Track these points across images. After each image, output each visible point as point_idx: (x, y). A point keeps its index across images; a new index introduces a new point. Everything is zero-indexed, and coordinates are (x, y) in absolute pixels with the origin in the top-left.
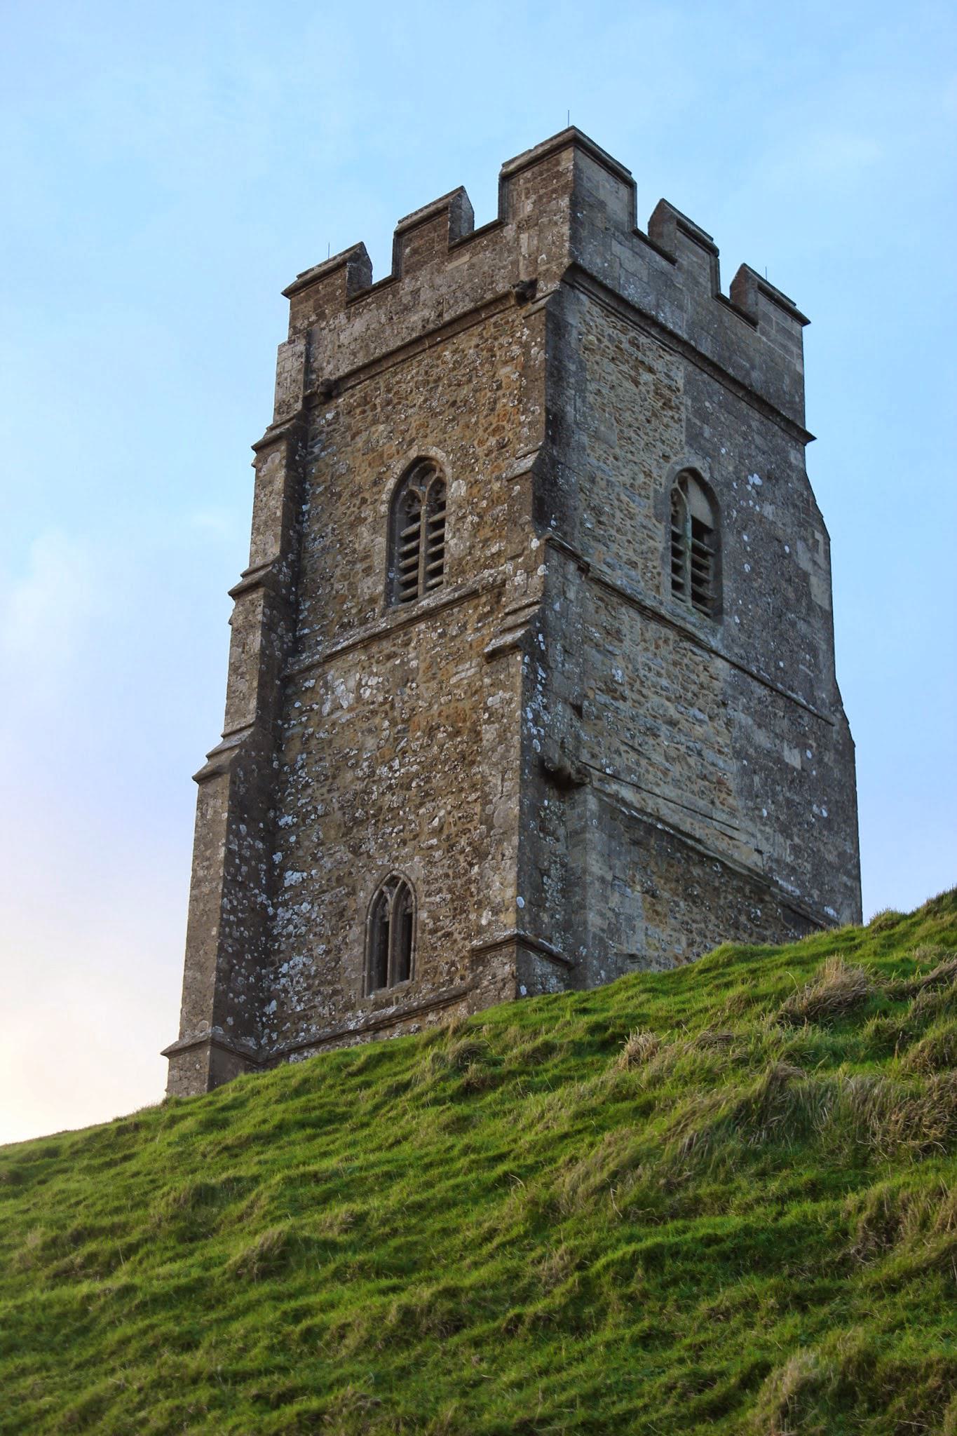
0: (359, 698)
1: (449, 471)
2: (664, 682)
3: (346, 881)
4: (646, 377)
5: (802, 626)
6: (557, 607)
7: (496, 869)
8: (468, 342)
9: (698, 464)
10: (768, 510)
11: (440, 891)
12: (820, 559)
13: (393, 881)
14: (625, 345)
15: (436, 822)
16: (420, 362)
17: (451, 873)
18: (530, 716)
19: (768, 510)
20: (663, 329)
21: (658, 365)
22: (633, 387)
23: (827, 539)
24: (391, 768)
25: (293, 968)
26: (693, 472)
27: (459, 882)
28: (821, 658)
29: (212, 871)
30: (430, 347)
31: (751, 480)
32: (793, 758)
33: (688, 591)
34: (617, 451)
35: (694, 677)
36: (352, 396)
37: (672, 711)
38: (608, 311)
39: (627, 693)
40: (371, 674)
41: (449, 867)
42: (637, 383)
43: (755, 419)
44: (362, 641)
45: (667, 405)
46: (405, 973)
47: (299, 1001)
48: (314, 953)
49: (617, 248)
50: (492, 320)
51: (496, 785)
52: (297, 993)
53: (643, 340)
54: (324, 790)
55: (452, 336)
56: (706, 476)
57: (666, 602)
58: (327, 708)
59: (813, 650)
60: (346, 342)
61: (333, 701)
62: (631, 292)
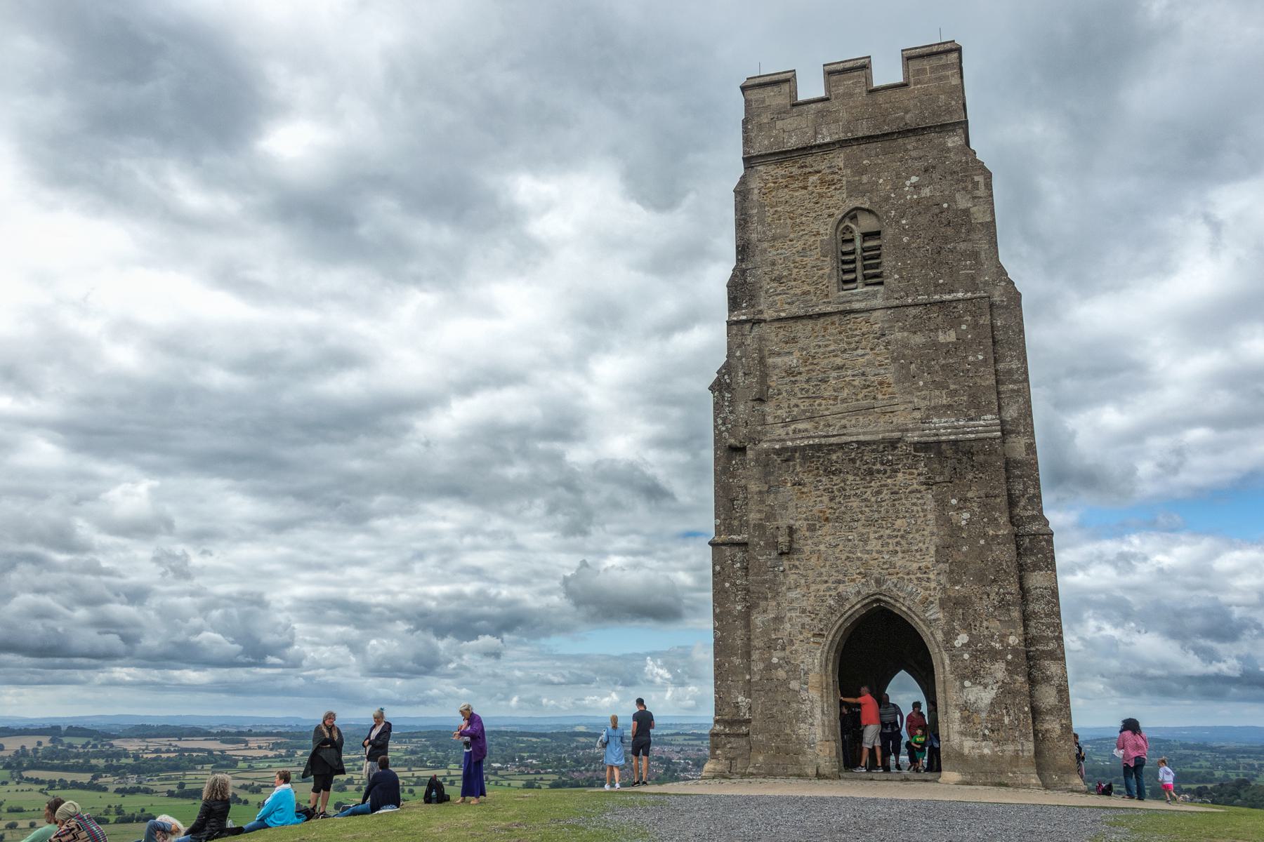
2: (832, 348)
4: (813, 179)
5: (962, 246)
6: (738, 354)
9: (857, 204)
10: (926, 192)
12: (981, 192)
14: (795, 171)
18: (720, 422)
19: (926, 192)
20: (819, 146)
21: (823, 166)
22: (804, 192)
23: (988, 175)
26: (857, 209)
28: (983, 255)
31: (908, 183)
32: (951, 336)
33: (860, 278)
34: (792, 236)
35: (857, 332)
37: (839, 361)
38: (779, 163)
39: (802, 369)
42: (805, 188)
43: (911, 143)
45: (832, 183)
49: (779, 124)
53: (809, 160)
56: (866, 206)
57: (836, 298)
59: (975, 255)
62: (793, 142)
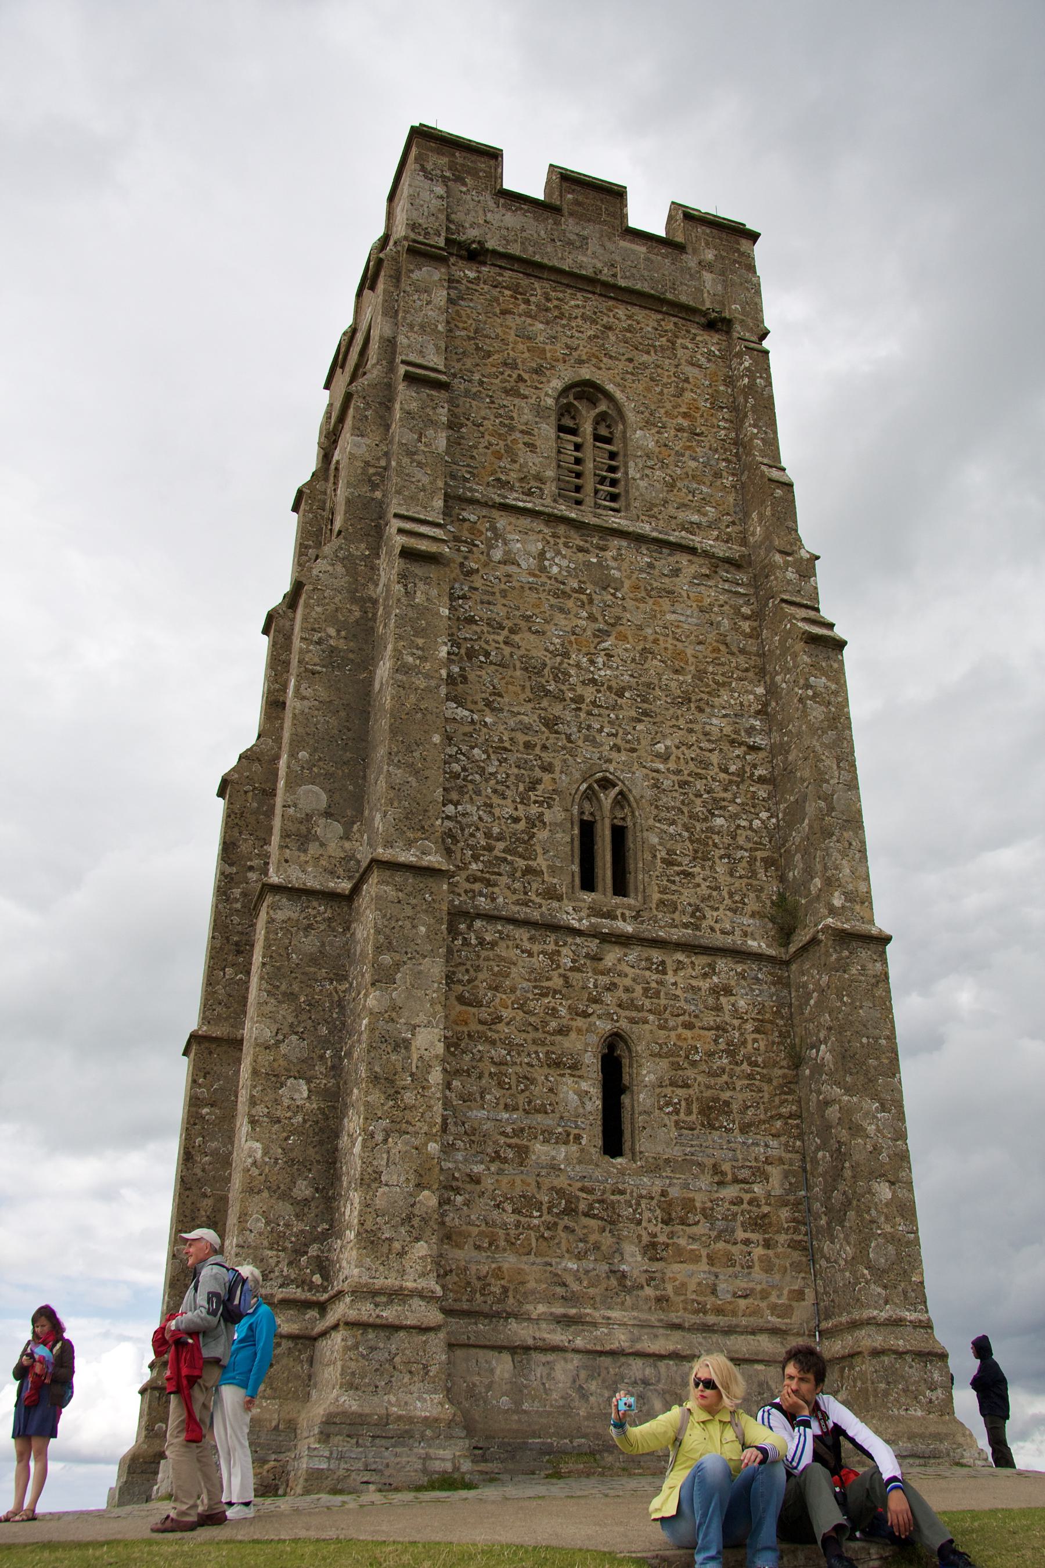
0: (543, 569)
1: (631, 417)
3: (537, 750)
7: (844, 854)
8: (648, 321)
11: (673, 823)
13: (606, 784)
15: (660, 747)
16: (586, 300)
17: (685, 810)
24: (592, 662)
25: (463, 815)
27: (698, 826)
29: (428, 666)
30: (601, 295)
36: (501, 275)
40: (558, 553)
41: (683, 802)
44: (549, 515)
46: (620, 888)
47: (476, 858)
48: (497, 811)
50: (676, 319)
51: (831, 768)
52: (472, 848)
54: (501, 639)
55: (627, 303)
58: (497, 554)
60: (496, 224)
61: (507, 553)
